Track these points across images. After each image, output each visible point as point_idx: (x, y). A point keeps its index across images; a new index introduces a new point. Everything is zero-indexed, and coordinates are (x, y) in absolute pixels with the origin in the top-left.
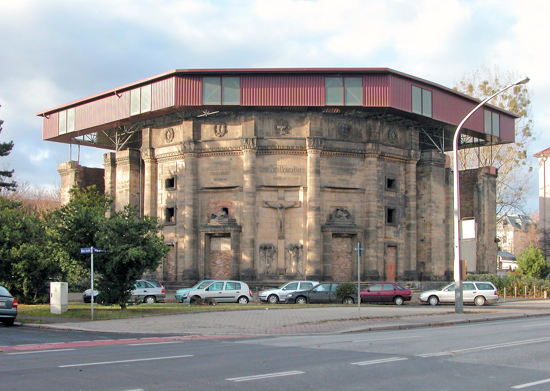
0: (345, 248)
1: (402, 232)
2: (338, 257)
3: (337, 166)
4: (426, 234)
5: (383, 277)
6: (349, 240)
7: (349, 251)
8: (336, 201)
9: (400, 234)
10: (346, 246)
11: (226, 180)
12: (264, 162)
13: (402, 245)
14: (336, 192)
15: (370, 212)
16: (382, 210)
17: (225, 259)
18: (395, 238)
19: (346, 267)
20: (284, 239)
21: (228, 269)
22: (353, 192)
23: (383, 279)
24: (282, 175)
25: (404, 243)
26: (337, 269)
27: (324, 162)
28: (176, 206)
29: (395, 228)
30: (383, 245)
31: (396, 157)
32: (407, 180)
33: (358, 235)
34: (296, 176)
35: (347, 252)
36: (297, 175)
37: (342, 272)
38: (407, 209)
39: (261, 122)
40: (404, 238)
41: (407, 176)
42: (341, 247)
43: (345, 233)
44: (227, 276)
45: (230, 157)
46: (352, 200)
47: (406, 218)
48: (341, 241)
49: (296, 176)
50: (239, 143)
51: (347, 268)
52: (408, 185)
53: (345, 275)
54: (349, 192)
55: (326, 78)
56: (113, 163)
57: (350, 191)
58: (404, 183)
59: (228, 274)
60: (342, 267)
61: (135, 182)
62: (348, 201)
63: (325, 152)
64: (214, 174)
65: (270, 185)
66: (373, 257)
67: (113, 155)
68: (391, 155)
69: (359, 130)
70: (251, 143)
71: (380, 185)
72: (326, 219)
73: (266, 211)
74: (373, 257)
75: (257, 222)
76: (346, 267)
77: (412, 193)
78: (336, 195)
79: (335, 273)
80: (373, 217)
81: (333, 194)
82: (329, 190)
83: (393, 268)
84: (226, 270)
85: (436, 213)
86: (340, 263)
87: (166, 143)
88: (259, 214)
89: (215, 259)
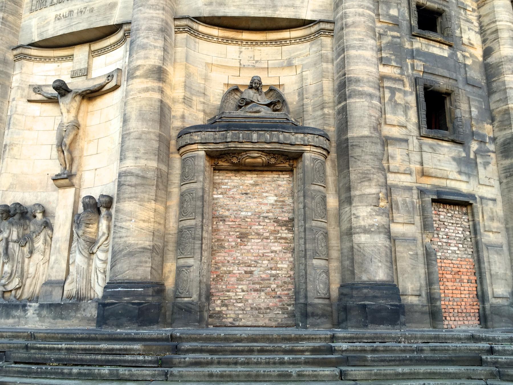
0: (268, 207)
1: (486, 164)
2: (243, 236)
5: (426, 309)
7: (285, 217)
9: (481, 168)
10: (272, 199)
13: (490, 203)
14: (242, 40)
15: (350, 80)
16: (401, 87)
18: (464, 178)
19: (274, 272)
20: (72, 185)
22: (295, 39)
23: (427, 318)
24: (75, 5)
25: (499, 199)
26: (239, 280)
29: (460, 148)
30: (415, 196)
32: (486, 20)
33: (306, 155)
35: (276, 221)
37: (256, 290)
38: (496, 97)
40: (496, 184)
41: (484, 11)
42: (252, 203)
43: (250, 146)
46: (296, 62)
47: (496, 124)
48: (256, 184)
51: (276, 276)
52: (489, 32)
53: (272, 302)
54: (285, 39)
58: (477, 29)
60: (257, 272)
62: (282, 67)
66: (366, 231)
71: (392, 17)
73: (37, 114)
74: (366, 231)
75: (4, 143)
76: (274, 272)
78: (241, 52)
79: (231, 294)
80: (361, 94)
82: (215, 31)
83: (465, 278)
86: (249, 258)
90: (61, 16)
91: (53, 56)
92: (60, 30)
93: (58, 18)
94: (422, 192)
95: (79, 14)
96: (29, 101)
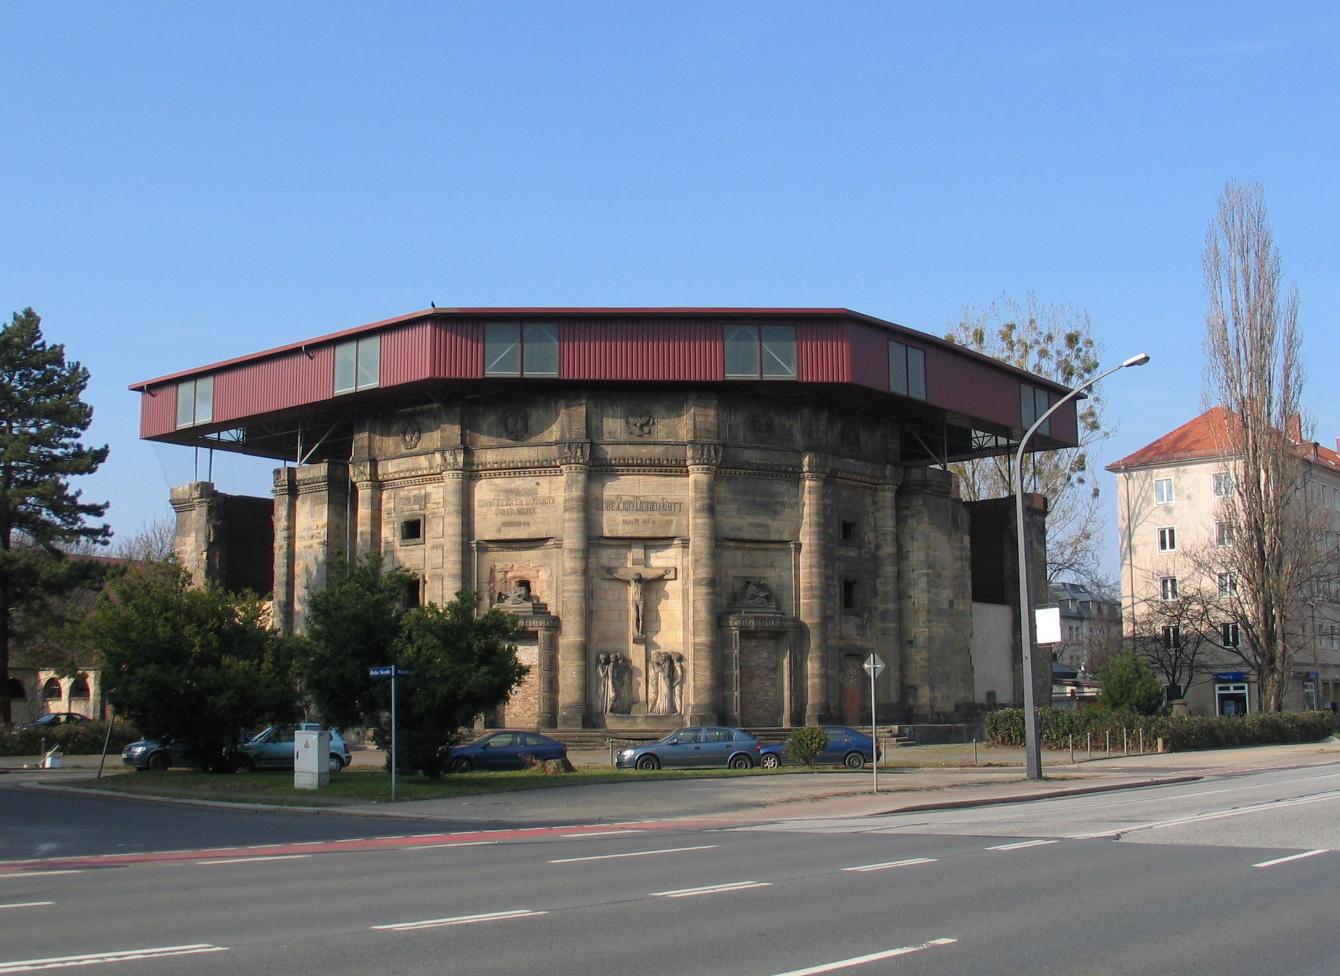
3: (747, 498)
4: (917, 630)
6: (771, 643)
7: (772, 666)
8: (744, 566)
10: (765, 655)
18: (859, 638)
27: (723, 491)
28: (424, 576)
31: (859, 478)
34: (668, 518)
36: (668, 515)
39: (599, 411)
48: (756, 647)
49: (668, 518)
50: (554, 451)
55: (726, 327)
56: (293, 490)
57: (771, 546)
60: (758, 698)
61: (338, 527)
63: (723, 471)
64: (503, 512)
65: (615, 535)
67: (291, 472)
68: (849, 475)
69: (788, 426)
70: (579, 453)
72: (725, 601)
77: (888, 549)
81: (739, 553)
82: (732, 544)
85: (936, 587)
87: (403, 450)
88: (595, 594)
93: (625, 522)
94: (840, 650)
96: (604, 579)
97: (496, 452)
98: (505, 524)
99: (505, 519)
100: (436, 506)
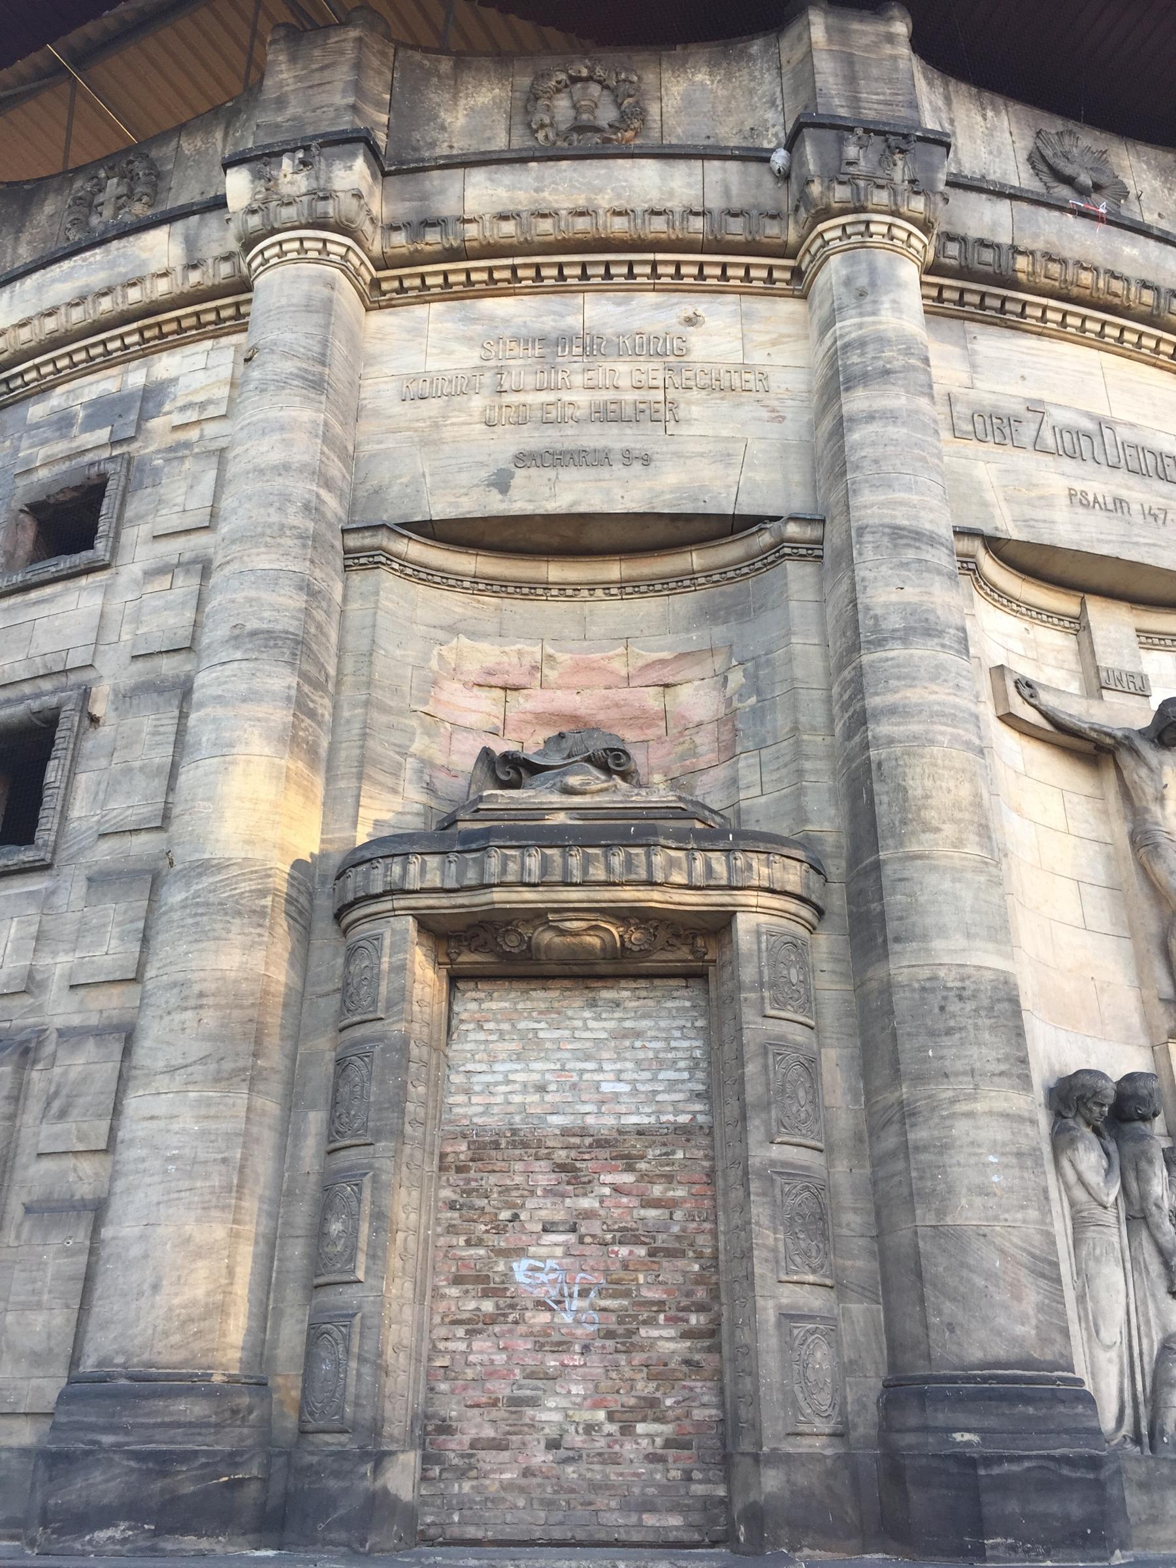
11: (646, 460)
12: (974, 366)
17: (628, 1236)
21: (660, 1373)
44: (652, 1458)
45: (688, 305)
59: (667, 1429)
84: (644, 1388)
89: (499, 1229)
90: (1091, 498)
91: (1017, 595)
92: (1099, 541)
93: (1078, 500)
95: (1150, 519)
97: (507, 176)
98: (524, 459)
99: (534, 439)
100: (192, 416)
